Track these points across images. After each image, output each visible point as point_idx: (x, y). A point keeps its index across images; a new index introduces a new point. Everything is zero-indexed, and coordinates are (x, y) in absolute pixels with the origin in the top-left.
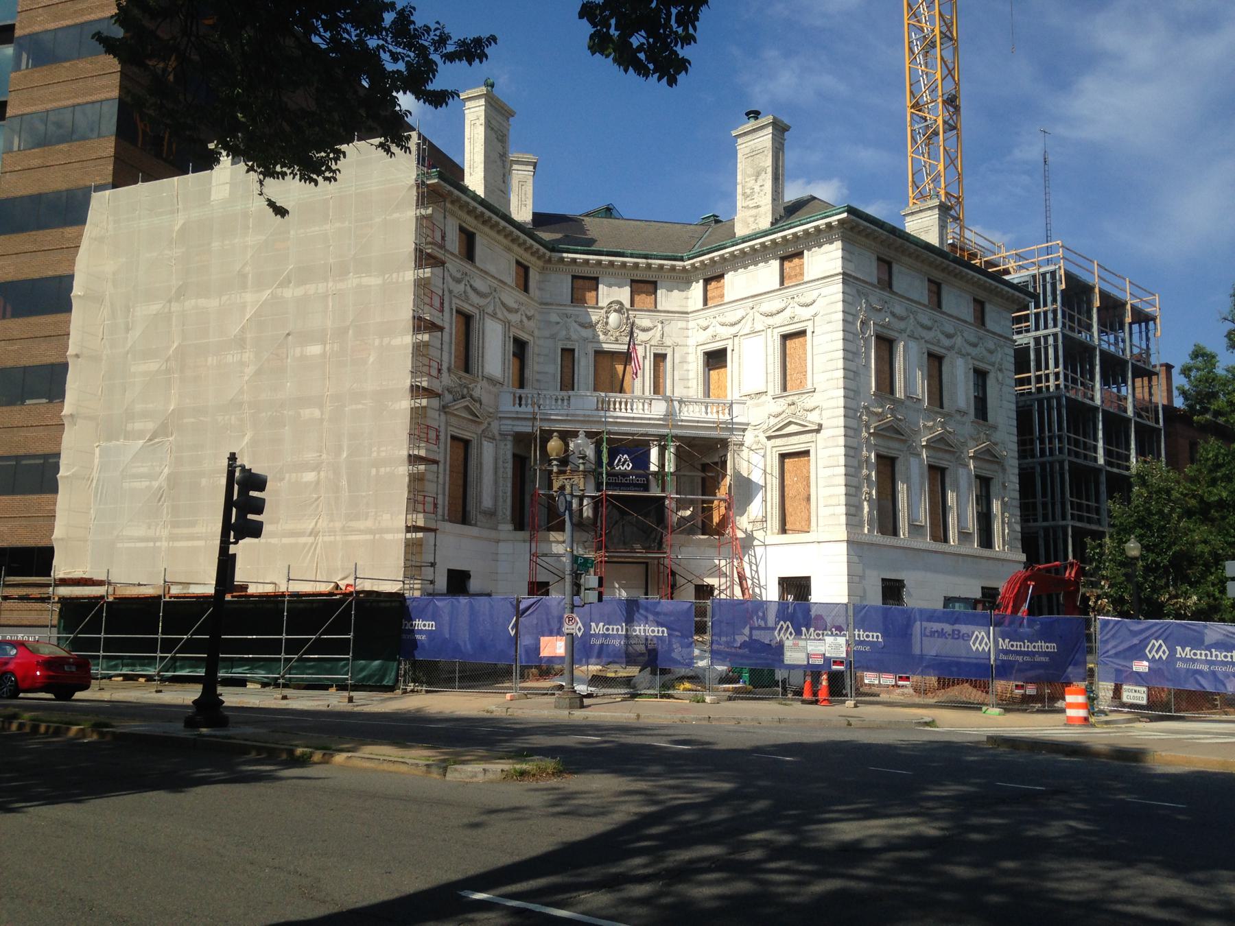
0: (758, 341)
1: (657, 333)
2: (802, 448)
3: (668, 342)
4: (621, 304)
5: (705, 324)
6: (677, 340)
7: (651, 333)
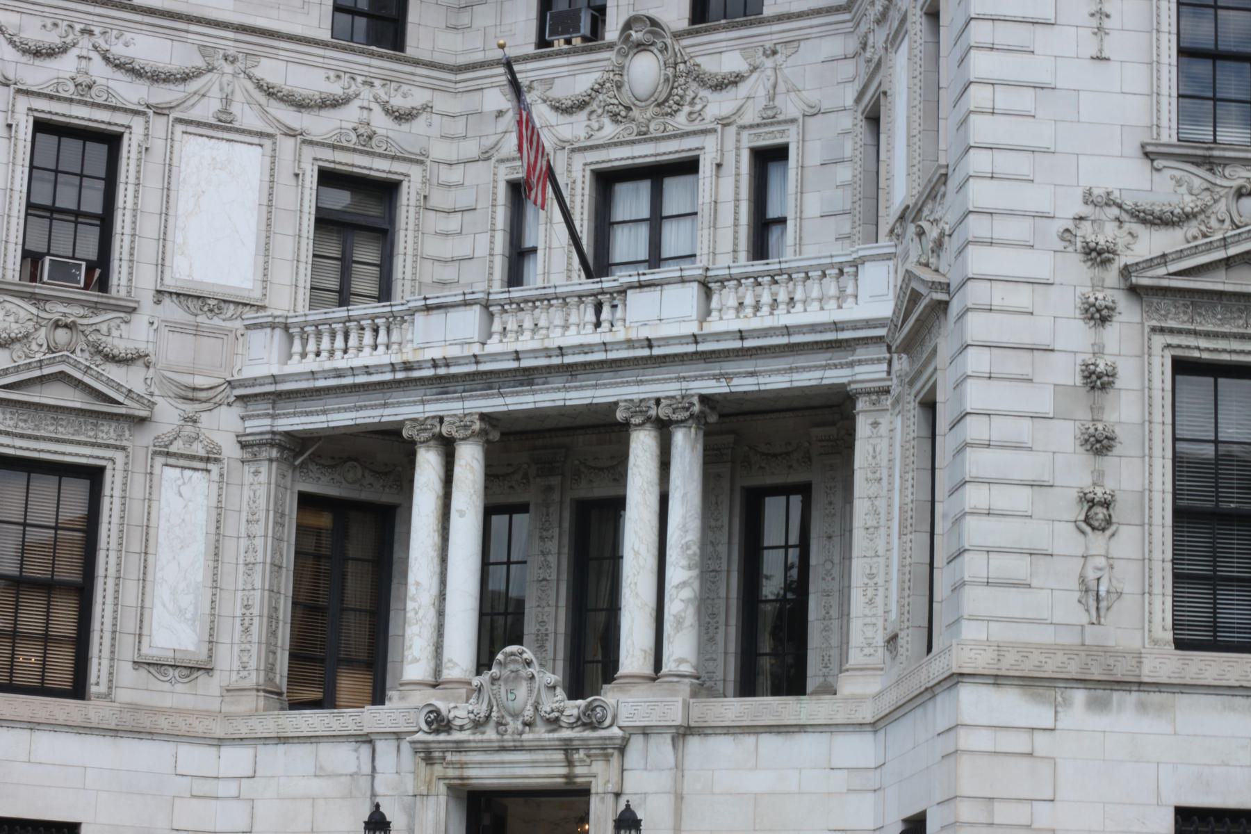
1: (755, 87)
3: (790, 107)
4: (653, 22)
6: (813, 96)
7: (743, 89)
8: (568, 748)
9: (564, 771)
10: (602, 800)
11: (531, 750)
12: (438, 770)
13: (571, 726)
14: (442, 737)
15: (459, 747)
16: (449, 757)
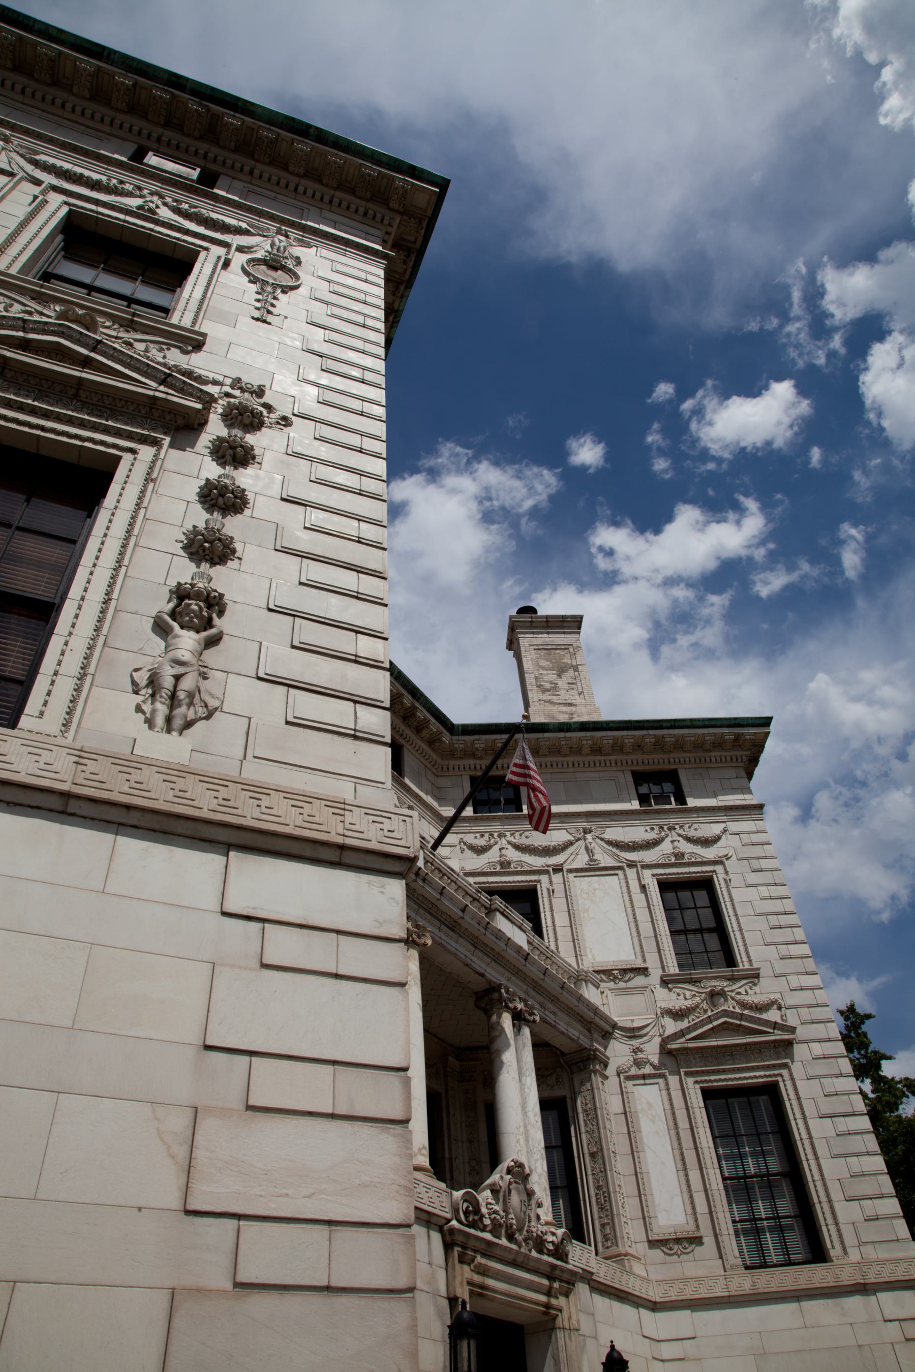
0: (612, 883)
2: (757, 1077)
5: (482, 842)
8: (551, 1274)
9: (543, 1298)
10: (570, 1335)
11: (528, 1270)
12: (466, 1272)
13: (550, 1253)
14: (472, 1231)
15: (488, 1250)
16: (479, 1259)
